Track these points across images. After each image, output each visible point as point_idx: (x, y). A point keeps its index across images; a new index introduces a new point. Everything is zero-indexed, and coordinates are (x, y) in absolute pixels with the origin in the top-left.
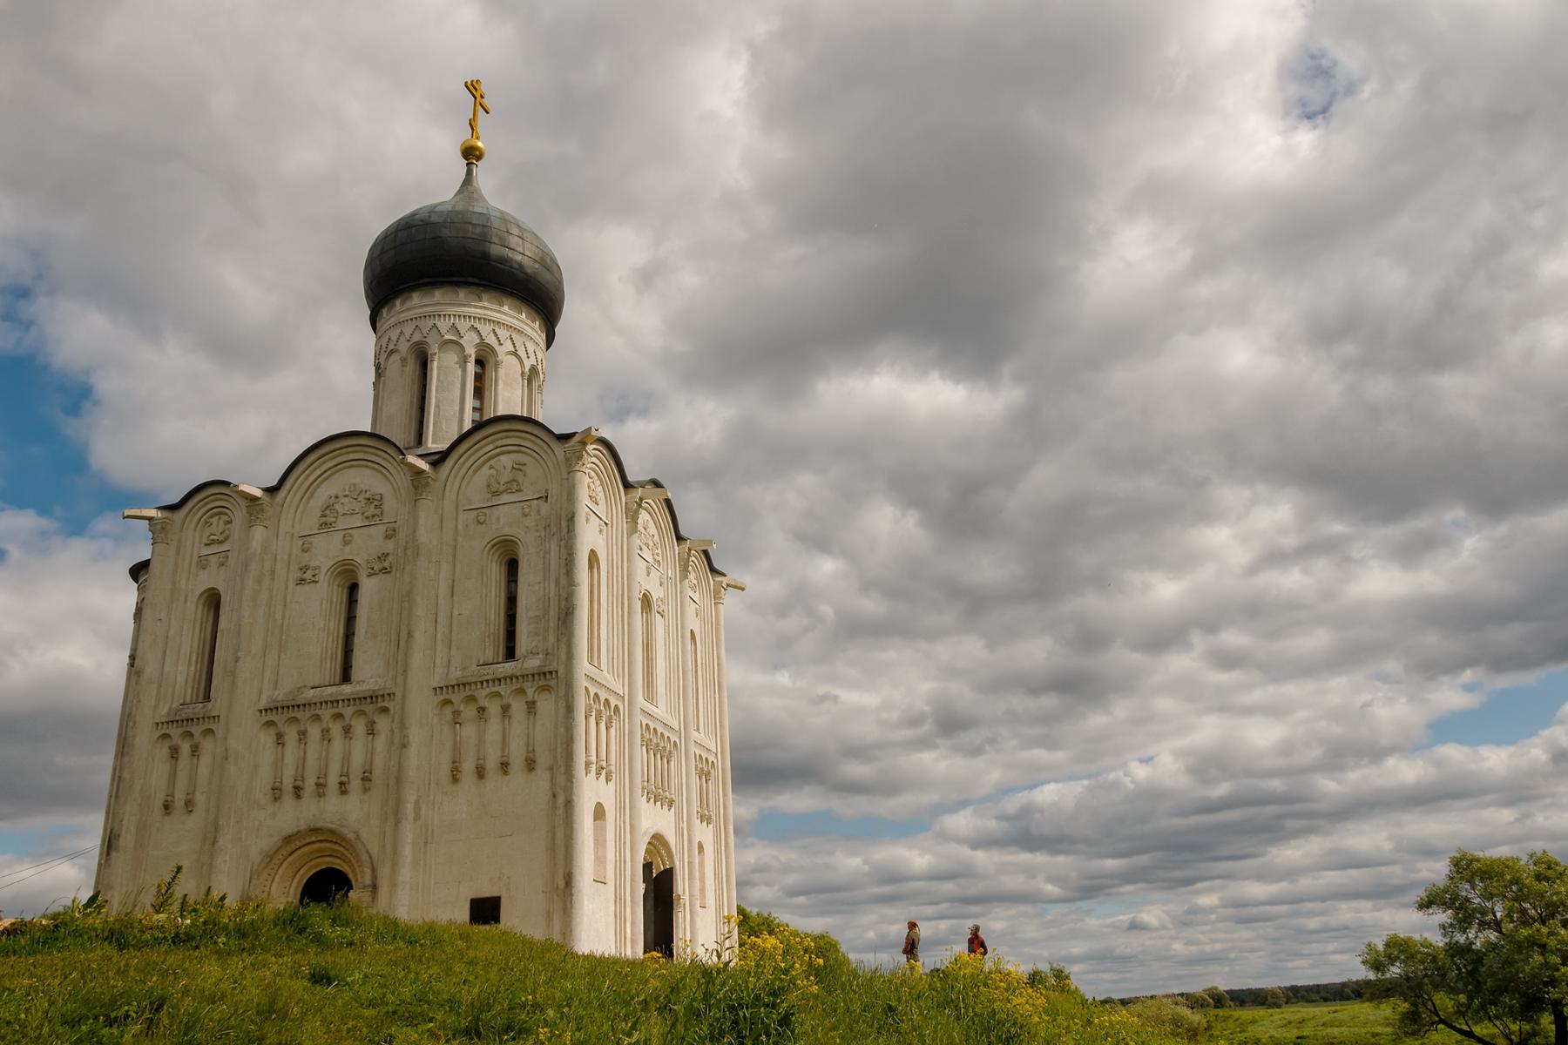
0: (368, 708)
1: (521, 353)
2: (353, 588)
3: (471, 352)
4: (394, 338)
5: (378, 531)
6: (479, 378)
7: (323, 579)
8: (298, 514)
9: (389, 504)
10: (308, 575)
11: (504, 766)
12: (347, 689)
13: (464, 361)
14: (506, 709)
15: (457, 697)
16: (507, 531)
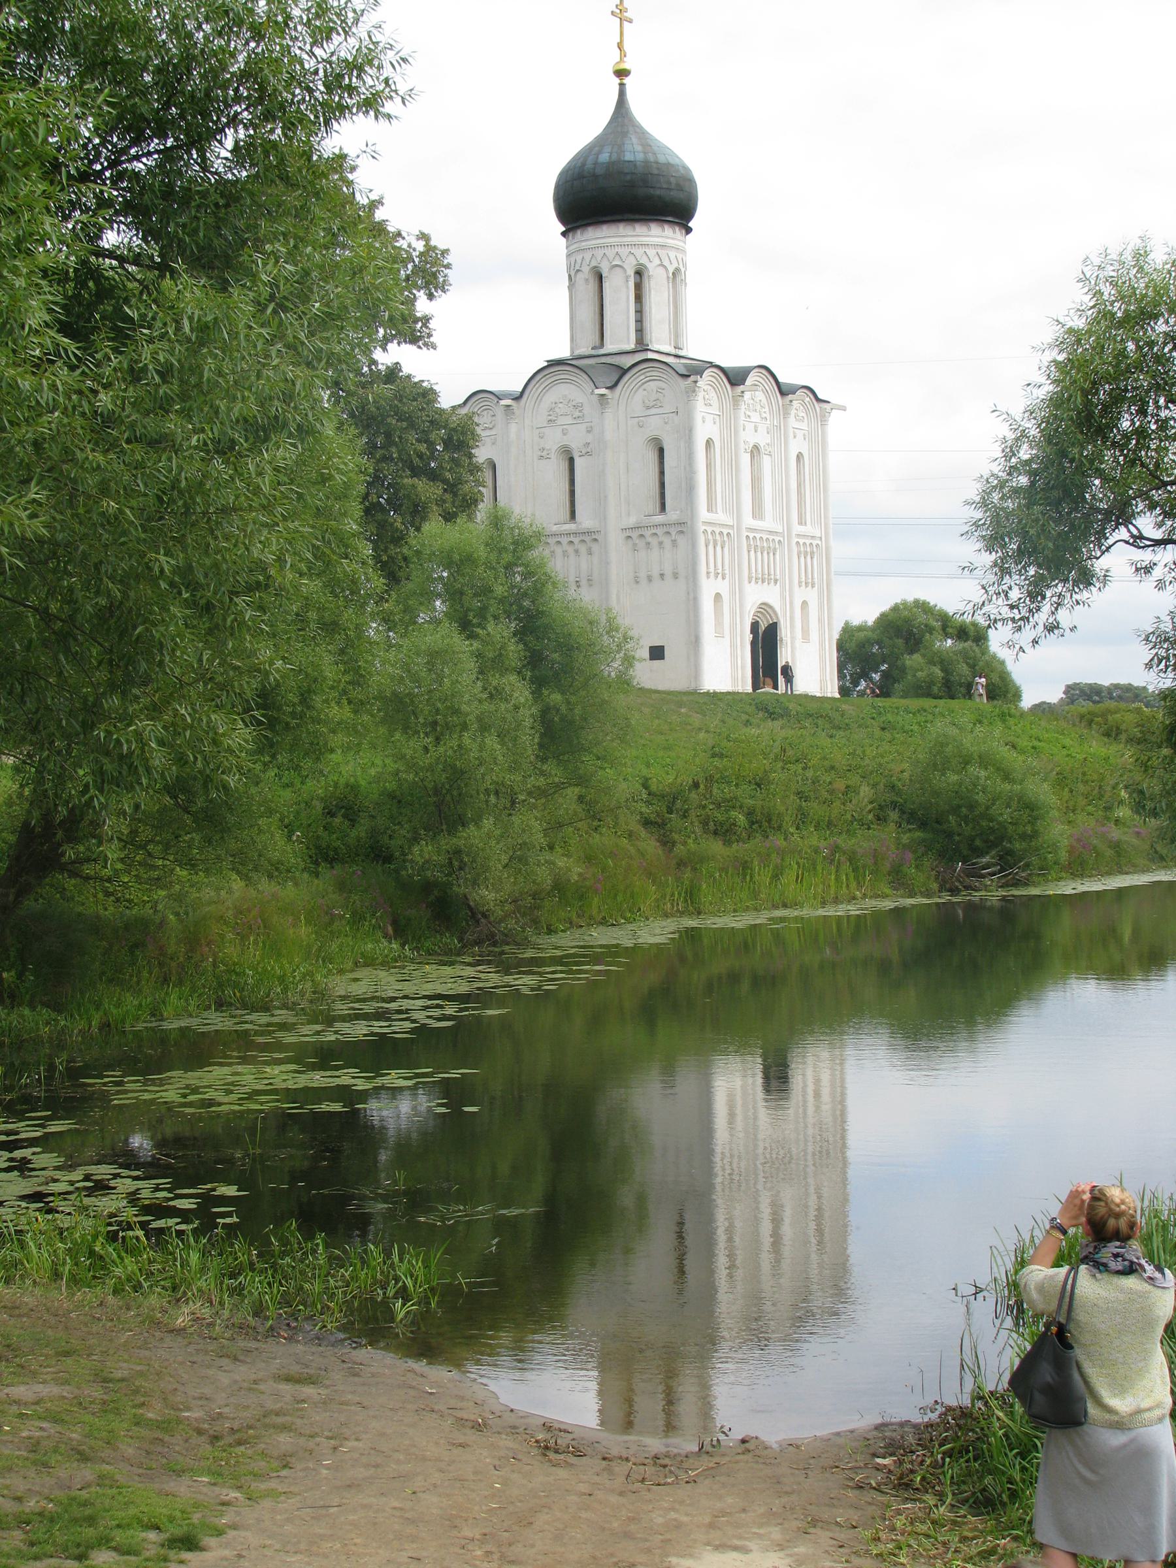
0: (587, 538)
1: (666, 263)
2: (571, 461)
3: (631, 272)
4: (579, 261)
5: (583, 427)
6: (638, 287)
7: (553, 456)
8: (533, 414)
9: (587, 410)
10: (544, 454)
11: (662, 575)
12: (572, 527)
13: (627, 278)
14: (661, 543)
15: (635, 535)
16: (655, 433)
